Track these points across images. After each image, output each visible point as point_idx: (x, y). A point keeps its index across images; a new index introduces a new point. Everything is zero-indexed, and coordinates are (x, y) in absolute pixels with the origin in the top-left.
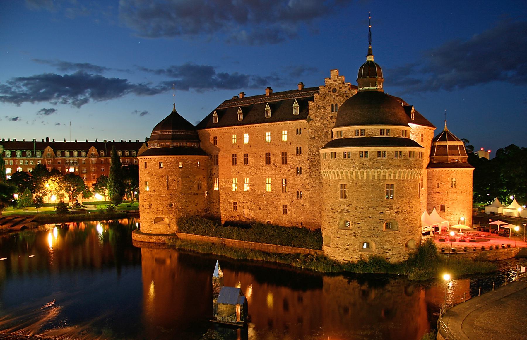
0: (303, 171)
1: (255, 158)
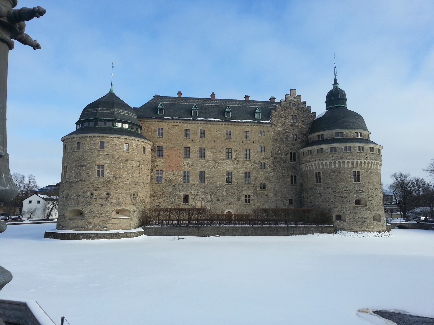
0: (266, 166)
1: (213, 153)
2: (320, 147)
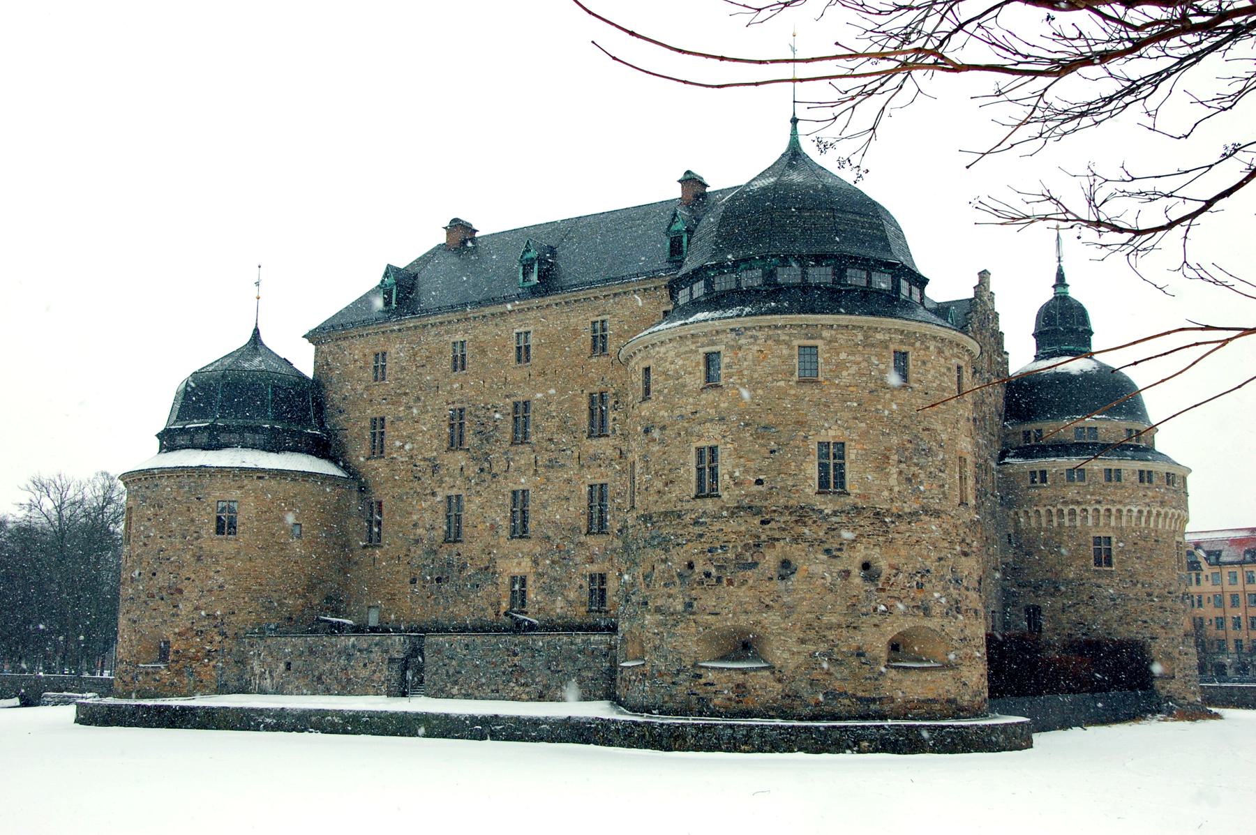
2: (1114, 464)
